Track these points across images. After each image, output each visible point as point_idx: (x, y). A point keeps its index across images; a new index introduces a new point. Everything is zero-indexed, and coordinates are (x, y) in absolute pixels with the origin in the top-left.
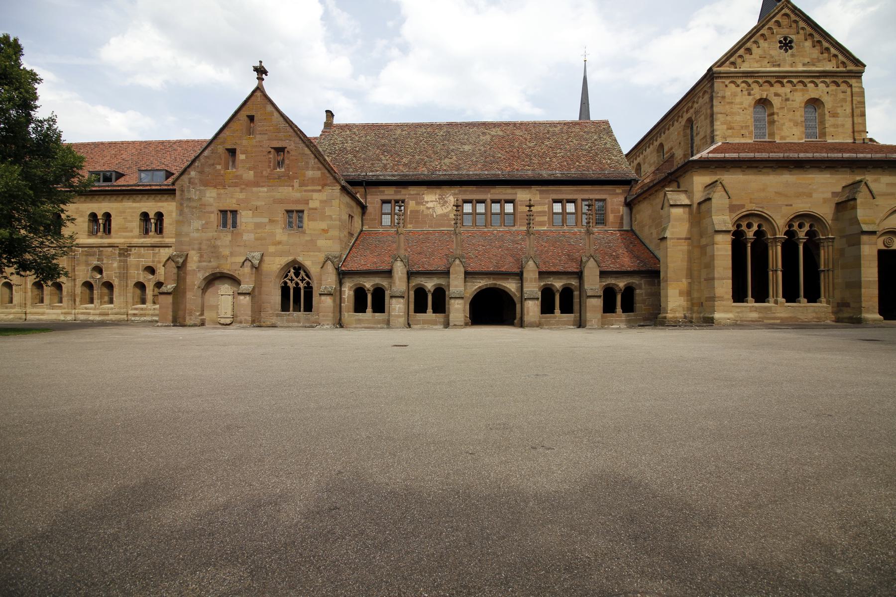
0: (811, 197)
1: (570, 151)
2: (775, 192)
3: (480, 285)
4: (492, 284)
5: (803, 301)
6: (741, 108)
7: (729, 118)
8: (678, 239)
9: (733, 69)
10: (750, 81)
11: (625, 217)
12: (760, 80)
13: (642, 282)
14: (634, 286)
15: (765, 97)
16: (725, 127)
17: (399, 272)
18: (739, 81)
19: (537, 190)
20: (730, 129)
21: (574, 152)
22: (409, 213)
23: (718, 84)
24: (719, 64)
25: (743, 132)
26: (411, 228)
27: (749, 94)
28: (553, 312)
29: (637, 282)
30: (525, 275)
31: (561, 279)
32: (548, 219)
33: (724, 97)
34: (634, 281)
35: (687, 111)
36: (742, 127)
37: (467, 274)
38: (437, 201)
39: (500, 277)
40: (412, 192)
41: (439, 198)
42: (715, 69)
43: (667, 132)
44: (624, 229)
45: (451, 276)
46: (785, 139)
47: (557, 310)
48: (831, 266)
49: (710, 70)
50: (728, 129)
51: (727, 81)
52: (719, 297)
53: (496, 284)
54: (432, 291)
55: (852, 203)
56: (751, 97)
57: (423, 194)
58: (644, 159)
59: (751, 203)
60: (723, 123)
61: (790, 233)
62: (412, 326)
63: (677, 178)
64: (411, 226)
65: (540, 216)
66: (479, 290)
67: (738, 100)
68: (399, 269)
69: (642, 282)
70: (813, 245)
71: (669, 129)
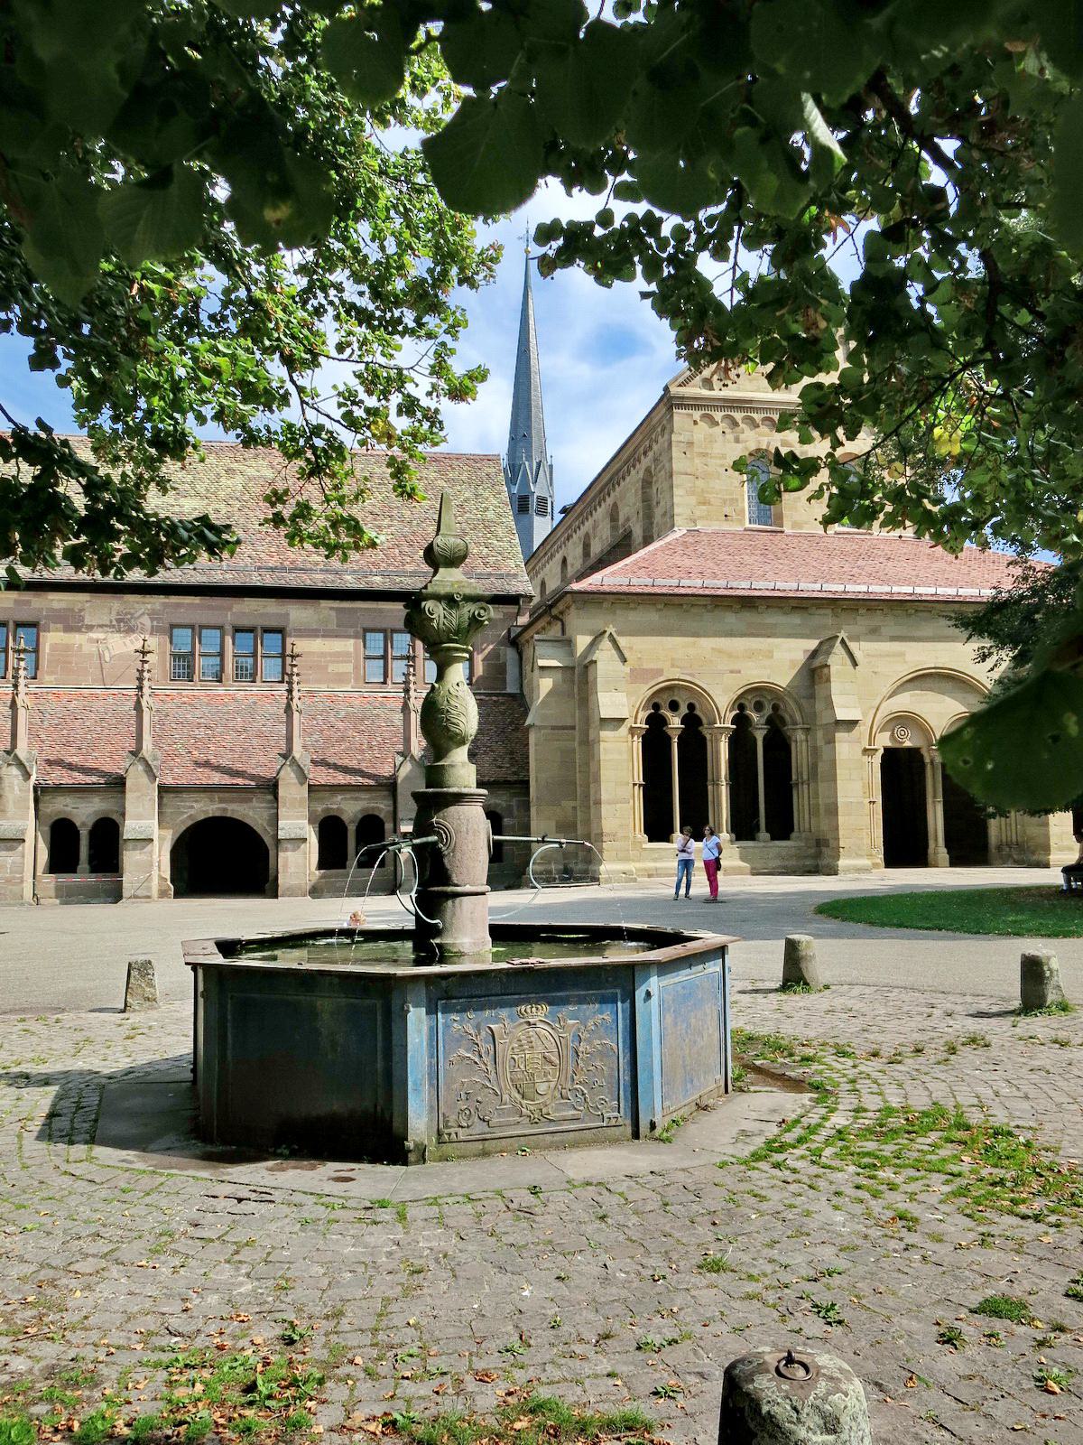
0: (772, 657)
1: (410, 522)
2: (713, 649)
3: (192, 812)
4: (218, 808)
5: (764, 835)
6: (722, 466)
7: (700, 483)
8: (554, 728)
9: (706, 393)
10: (738, 416)
11: (509, 668)
12: (755, 415)
13: (514, 802)
14: (498, 810)
15: (764, 447)
16: (693, 500)
17: (16, 788)
18: (718, 415)
19: (331, 608)
20: (704, 504)
21: (418, 525)
22: (47, 651)
23: (680, 416)
24: (681, 380)
25: (728, 510)
26: (51, 682)
27: (737, 440)
28: (343, 866)
29: (504, 804)
30: (281, 792)
31: (356, 799)
32: (356, 668)
33: (690, 444)
34: (497, 801)
35: (645, 453)
36: (725, 501)
37: (163, 790)
38: (114, 626)
39: (235, 795)
40: (56, 605)
41: (117, 620)
42: (674, 390)
43: (622, 483)
44: (509, 690)
45: (129, 795)
46: (801, 528)
47: (353, 862)
48: (805, 777)
49: (666, 389)
50: (700, 503)
51: (697, 414)
52: (609, 835)
53: (225, 810)
54: (90, 823)
55: (825, 670)
56: (740, 446)
57: (81, 610)
58: (595, 528)
59: (673, 666)
60: (691, 492)
61: (741, 720)
62: (42, 901)
63: (562, 613)
64: (52, 678)
65: (338, 662)
66: (190, 823)
67: (717, 448)
68: (16, 782)
69: (514, 802)
70: (779, 744)
71: (624, 479)
